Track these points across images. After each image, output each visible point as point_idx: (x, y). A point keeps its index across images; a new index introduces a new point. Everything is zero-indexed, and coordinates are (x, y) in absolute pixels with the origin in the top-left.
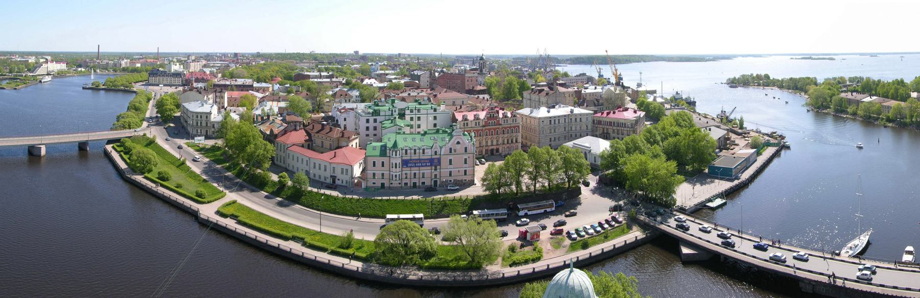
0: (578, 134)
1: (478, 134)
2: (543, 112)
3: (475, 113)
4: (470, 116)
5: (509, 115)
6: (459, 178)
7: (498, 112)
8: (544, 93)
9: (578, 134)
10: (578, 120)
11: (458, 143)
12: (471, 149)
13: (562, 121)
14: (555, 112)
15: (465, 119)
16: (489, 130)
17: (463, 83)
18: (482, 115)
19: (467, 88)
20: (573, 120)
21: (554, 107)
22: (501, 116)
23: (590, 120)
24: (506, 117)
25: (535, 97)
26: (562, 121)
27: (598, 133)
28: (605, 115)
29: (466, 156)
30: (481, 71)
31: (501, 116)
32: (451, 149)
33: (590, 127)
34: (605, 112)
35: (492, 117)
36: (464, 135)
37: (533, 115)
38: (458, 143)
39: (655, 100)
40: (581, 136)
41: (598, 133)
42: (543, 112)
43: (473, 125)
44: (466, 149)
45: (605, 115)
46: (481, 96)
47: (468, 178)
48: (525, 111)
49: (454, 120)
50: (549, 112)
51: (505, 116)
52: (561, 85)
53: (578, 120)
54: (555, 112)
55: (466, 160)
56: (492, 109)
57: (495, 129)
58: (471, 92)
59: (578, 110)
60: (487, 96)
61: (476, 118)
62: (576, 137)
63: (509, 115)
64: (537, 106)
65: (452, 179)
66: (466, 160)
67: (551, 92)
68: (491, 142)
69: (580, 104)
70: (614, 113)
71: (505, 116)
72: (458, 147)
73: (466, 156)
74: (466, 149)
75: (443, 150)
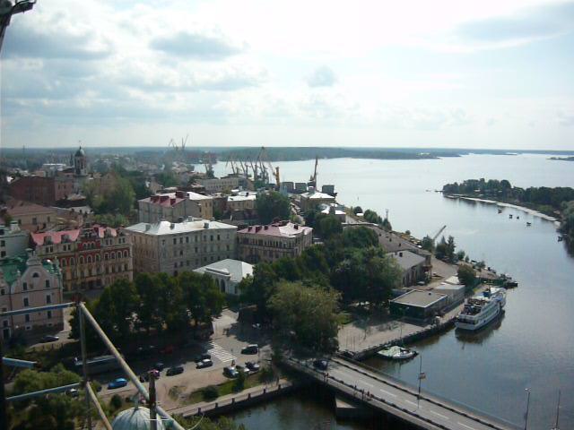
0: (215, 257)
1: (65, 260)
2: (164, 228)
3: (62, 233)
4: (56, 238)
5: (114, 233)
6: (41, 323)
7: (97, 230)
8: (168, 204)
9: (215, 257)
10: (215, 238)
11: (36, 275)
12: (56, 282)
13: (192, 239)
14: (181, 228)
15: (47, 242)
16: (85, 255)
17: (51, 191)
18: (74, 235)
19: (57, 199)
20: (208, 237)
21: (180, 221)
22: (101, 235)
23: (233, 237)
24: (110, 236)
25: (156, 207)
26: (192, 239)
27: (244, 256)
28: (253, 231)
29: (49, 293)
30: (78, 172)
31: (101, 235)
32: (25, 285)
33: (231, 247)
34: (254, 228)
35: (88, 237)
36: (45, 263)
37: (151, 232)
38: (36, 275)
39: (332, 210)
40: (219, 260)
41: (244, 256)
42: (164, 228)
43: (61, 250)
44: (47, 282)
45: (253, 231)
46: (77, 209)
47: (52, 322)
48: (140, 228)
49: (32, 244)
50: (172, 227)
51: (107, 235)
52: (197, 191)
53: (215, 238)
54: (181, 228)
55: (48, 298)
56: (88, 226)
57: (93, 254)
58: (64, 203)
59: (214, 225)
60: (86, 209)
61: (65, 240)
62: (212, 261)
63: (114, 233)
64: (154, 219)
65: (30, 325)
66: (48, 298)
67: (178, 200)
68: (86, 271)
69: (217, 217)
70: (266, 228)
71: (107, 235)
72: (36, 280)
73: (49, 293)
74: (47, 282)
75: (13, 286)
